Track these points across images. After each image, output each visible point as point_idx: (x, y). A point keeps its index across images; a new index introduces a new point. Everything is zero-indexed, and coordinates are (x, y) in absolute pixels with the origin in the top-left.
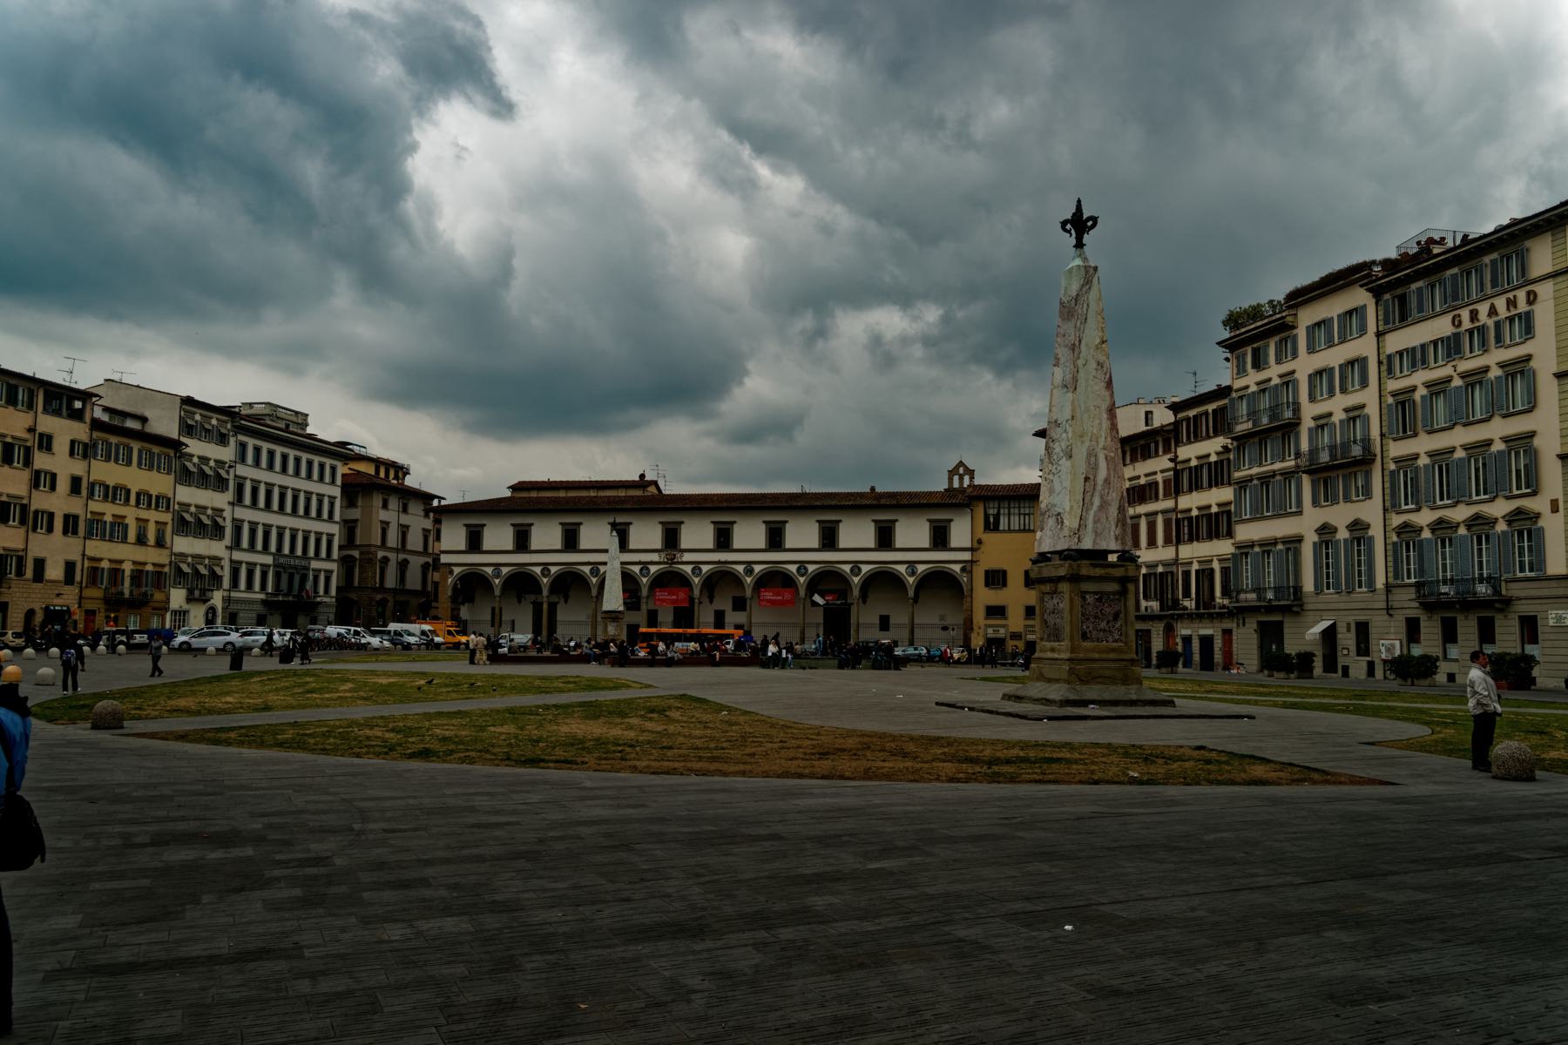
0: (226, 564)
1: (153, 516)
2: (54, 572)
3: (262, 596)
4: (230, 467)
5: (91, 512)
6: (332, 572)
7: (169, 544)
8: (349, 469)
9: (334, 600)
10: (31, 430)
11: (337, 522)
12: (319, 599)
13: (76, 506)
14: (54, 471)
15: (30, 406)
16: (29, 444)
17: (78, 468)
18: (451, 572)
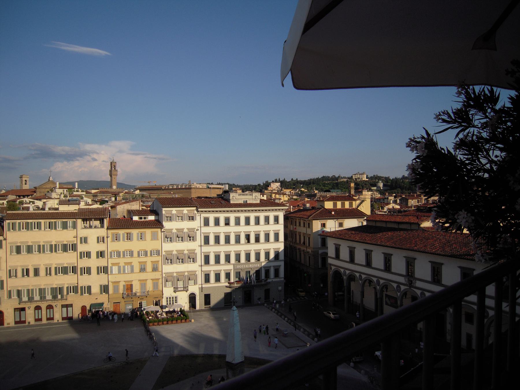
0: (199, 274)
1: (149, 260)
2: (95, 290)
3: (227, 284)
4: (197, 230)
6: (280, 266)
7: (160, 270)
8: (321, 205)
9: (283, 279)
11: (281, 242)
12: (269, 280)
13: (102, 262)
14: (89, 251)
15: (75, 226)
16: (75, 242)
18: (331, 268)
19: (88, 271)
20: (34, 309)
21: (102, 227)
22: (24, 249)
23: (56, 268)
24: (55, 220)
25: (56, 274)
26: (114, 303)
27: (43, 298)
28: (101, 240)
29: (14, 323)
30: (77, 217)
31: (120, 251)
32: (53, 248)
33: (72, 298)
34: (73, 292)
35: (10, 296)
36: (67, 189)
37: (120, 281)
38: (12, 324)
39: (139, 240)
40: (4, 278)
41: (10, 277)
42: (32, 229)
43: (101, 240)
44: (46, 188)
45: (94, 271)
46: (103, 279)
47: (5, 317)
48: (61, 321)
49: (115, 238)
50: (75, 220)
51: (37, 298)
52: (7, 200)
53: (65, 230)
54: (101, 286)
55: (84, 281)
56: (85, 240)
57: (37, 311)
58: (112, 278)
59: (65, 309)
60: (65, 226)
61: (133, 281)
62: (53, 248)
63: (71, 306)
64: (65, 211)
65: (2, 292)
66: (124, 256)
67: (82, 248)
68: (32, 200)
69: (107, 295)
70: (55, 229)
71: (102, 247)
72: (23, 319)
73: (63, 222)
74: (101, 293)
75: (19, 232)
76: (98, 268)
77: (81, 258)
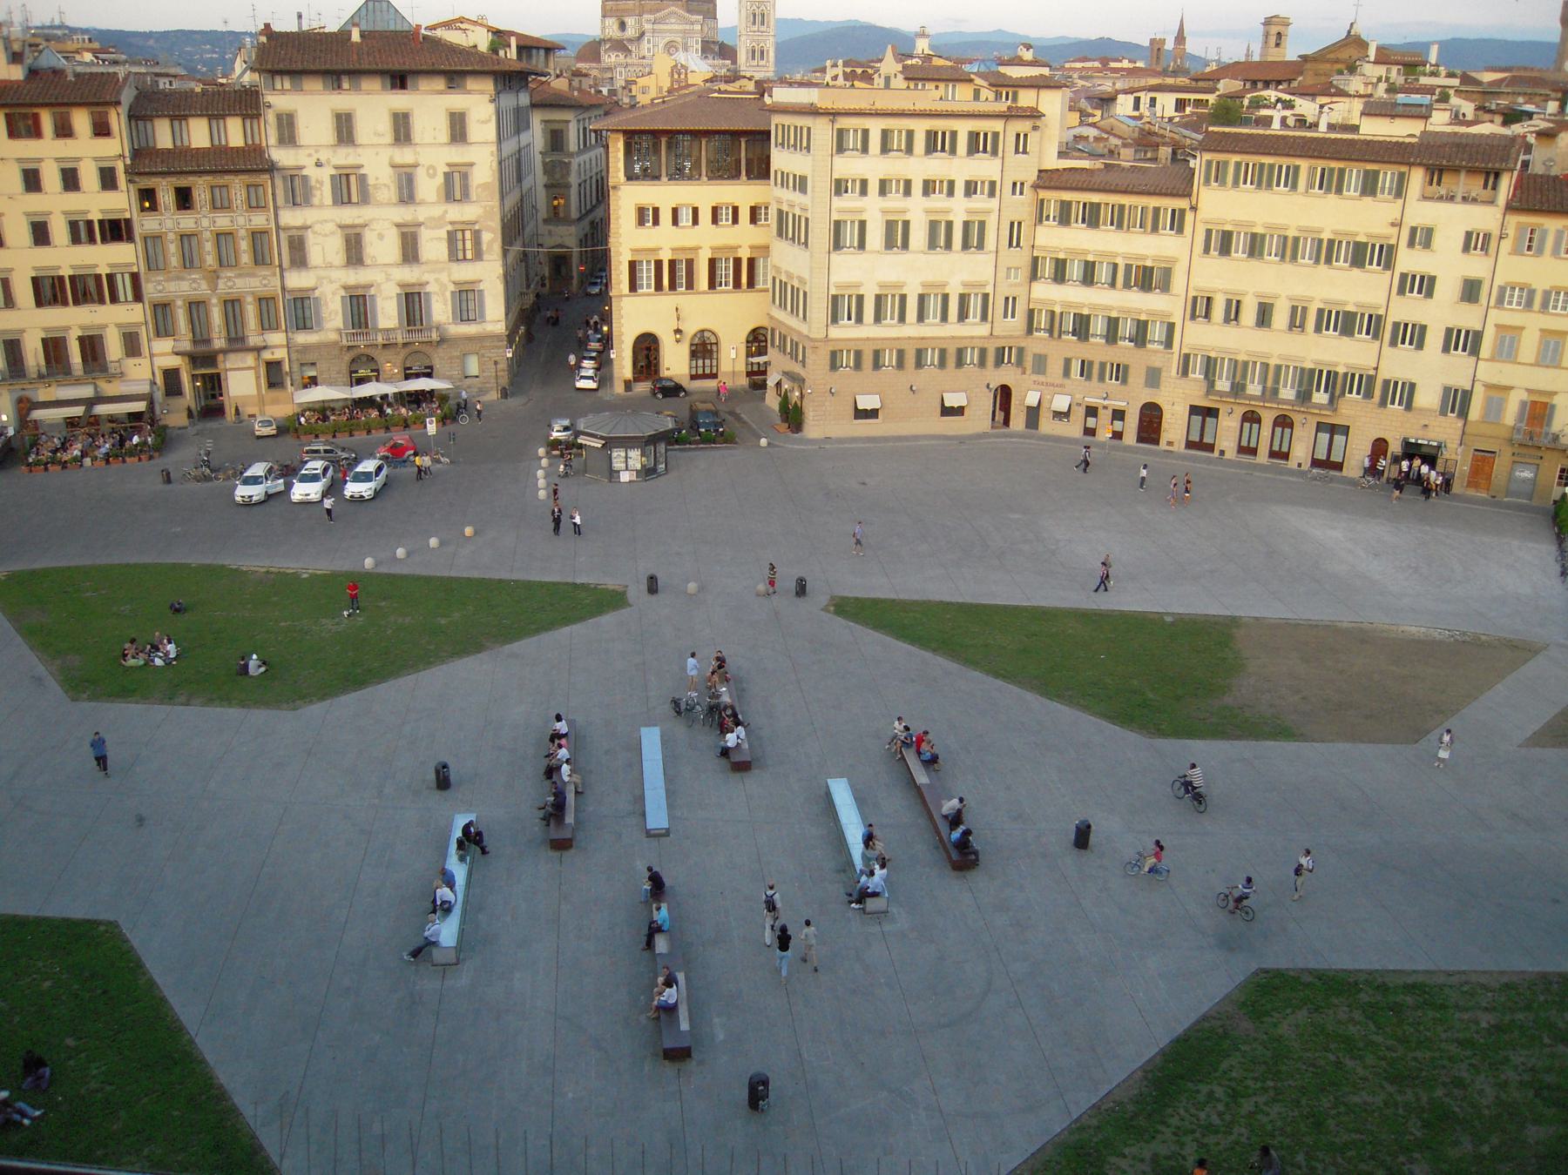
2: (1428, 397)
5: (1497, 326)
10: (1397, 225)
13: (1468, 318)
15: (1399, 191)
16: (1393, 241)
17: (1476, 267)
19: (1414, 335)
20: (1240, 419)
21: (1492, 202)
22: (1240, 244)
23: (1320, 312)
24: (1341, 165)
25: (1318, 329)
26: (1476, 450)
27: (1271, 393)
28: (1473, 242)
29: (1183, 446)
30: (1412, 160)
31: (1534, 287)
32: (1326, 252)
33: (1352, 409)
34: (1358, 393)
35: (1185, 373)
36: (1400, 67)
37: (1512, 388)
38: (1179, 447)
39: (1559, 254)
40: (1177, 319)
41: (1193, 317)
42: (1236, 183)
43: (1473, 242)
44: (1337, 61)
45: (1434, 339)
46: (1457, 370)
47: (1164, 425)
48: (1306, 466)
49: (1527, 244)
50: (1404, 169)
51: (1254, 389)
52: (1218, 93)
53: (1368, 200)
54: (1447, 390)
55: (1398, 364)
56: (1422, 238)
57: (1247, 425)
58: (1489, 372)
59: (1324, 437)
60: (1369, 187)
61: (1556, 393)
62: (1326, 252)
63: (1345, 430)
64: (1376, 138)
65: (1167, 356)
66: (1545, 305)
67: (1409, 261)
68: (1287, 97)
69: (1460, 424)
70: (1339, 191)
71: (1476, 267)
72: (1208, 440)
73: (1367, 172)
74: (1443, 413)
75: (1232, 192)
76: (1449, 331)
77: (1401, 291)
